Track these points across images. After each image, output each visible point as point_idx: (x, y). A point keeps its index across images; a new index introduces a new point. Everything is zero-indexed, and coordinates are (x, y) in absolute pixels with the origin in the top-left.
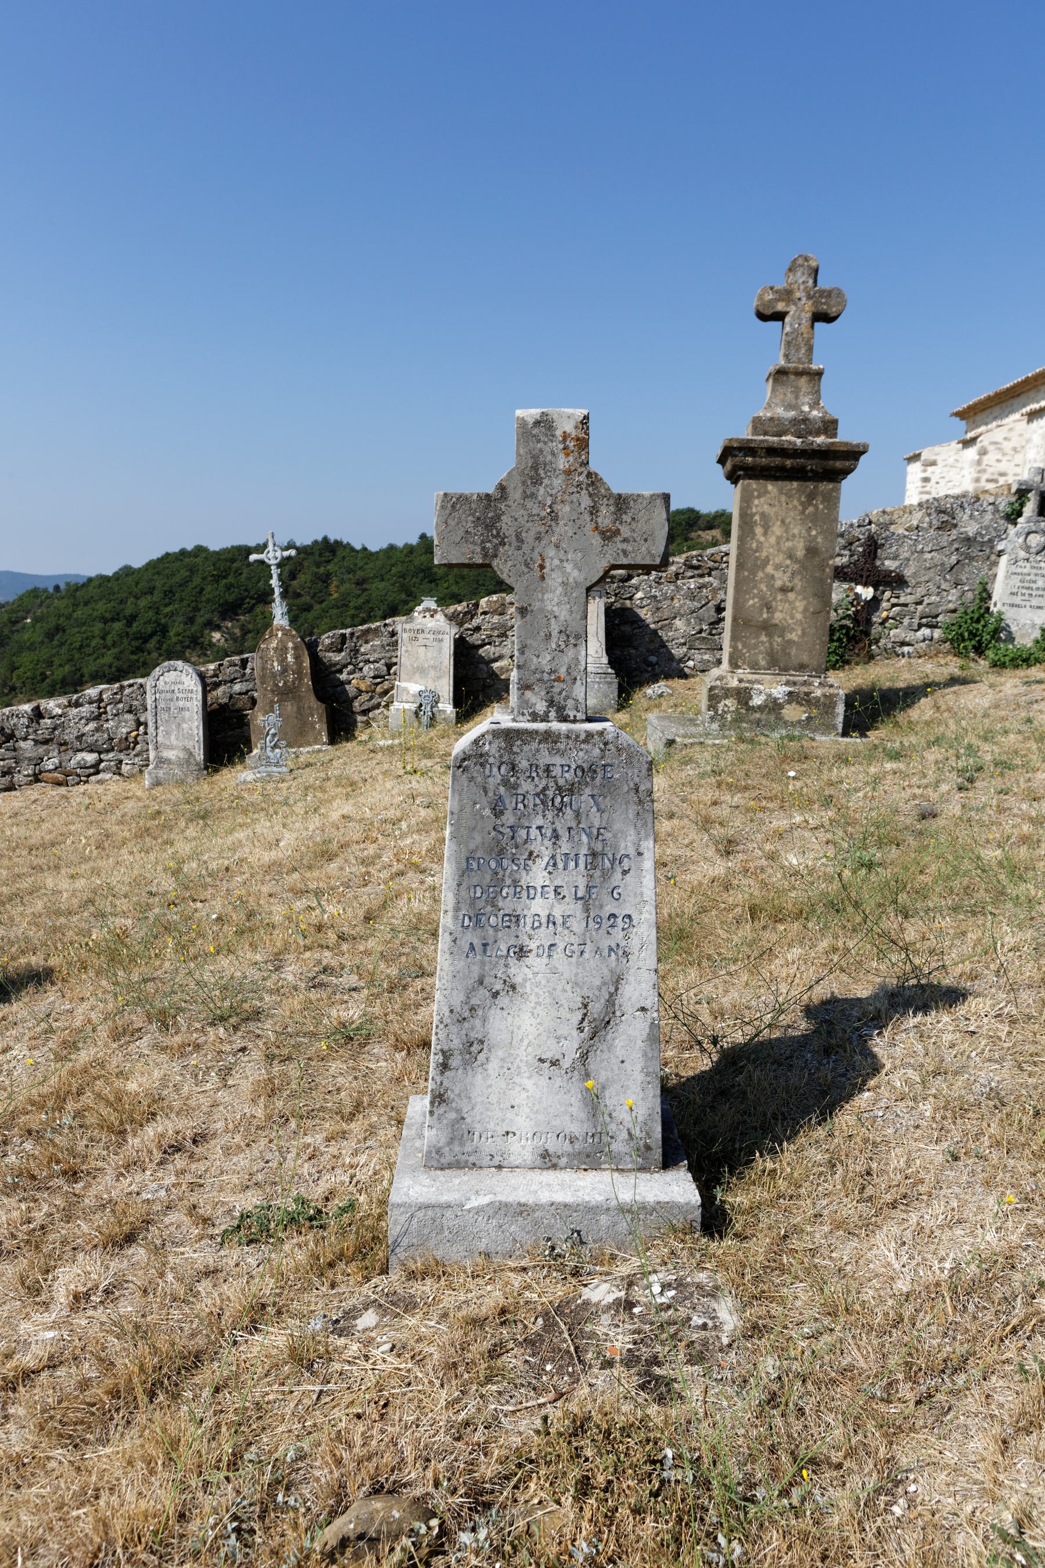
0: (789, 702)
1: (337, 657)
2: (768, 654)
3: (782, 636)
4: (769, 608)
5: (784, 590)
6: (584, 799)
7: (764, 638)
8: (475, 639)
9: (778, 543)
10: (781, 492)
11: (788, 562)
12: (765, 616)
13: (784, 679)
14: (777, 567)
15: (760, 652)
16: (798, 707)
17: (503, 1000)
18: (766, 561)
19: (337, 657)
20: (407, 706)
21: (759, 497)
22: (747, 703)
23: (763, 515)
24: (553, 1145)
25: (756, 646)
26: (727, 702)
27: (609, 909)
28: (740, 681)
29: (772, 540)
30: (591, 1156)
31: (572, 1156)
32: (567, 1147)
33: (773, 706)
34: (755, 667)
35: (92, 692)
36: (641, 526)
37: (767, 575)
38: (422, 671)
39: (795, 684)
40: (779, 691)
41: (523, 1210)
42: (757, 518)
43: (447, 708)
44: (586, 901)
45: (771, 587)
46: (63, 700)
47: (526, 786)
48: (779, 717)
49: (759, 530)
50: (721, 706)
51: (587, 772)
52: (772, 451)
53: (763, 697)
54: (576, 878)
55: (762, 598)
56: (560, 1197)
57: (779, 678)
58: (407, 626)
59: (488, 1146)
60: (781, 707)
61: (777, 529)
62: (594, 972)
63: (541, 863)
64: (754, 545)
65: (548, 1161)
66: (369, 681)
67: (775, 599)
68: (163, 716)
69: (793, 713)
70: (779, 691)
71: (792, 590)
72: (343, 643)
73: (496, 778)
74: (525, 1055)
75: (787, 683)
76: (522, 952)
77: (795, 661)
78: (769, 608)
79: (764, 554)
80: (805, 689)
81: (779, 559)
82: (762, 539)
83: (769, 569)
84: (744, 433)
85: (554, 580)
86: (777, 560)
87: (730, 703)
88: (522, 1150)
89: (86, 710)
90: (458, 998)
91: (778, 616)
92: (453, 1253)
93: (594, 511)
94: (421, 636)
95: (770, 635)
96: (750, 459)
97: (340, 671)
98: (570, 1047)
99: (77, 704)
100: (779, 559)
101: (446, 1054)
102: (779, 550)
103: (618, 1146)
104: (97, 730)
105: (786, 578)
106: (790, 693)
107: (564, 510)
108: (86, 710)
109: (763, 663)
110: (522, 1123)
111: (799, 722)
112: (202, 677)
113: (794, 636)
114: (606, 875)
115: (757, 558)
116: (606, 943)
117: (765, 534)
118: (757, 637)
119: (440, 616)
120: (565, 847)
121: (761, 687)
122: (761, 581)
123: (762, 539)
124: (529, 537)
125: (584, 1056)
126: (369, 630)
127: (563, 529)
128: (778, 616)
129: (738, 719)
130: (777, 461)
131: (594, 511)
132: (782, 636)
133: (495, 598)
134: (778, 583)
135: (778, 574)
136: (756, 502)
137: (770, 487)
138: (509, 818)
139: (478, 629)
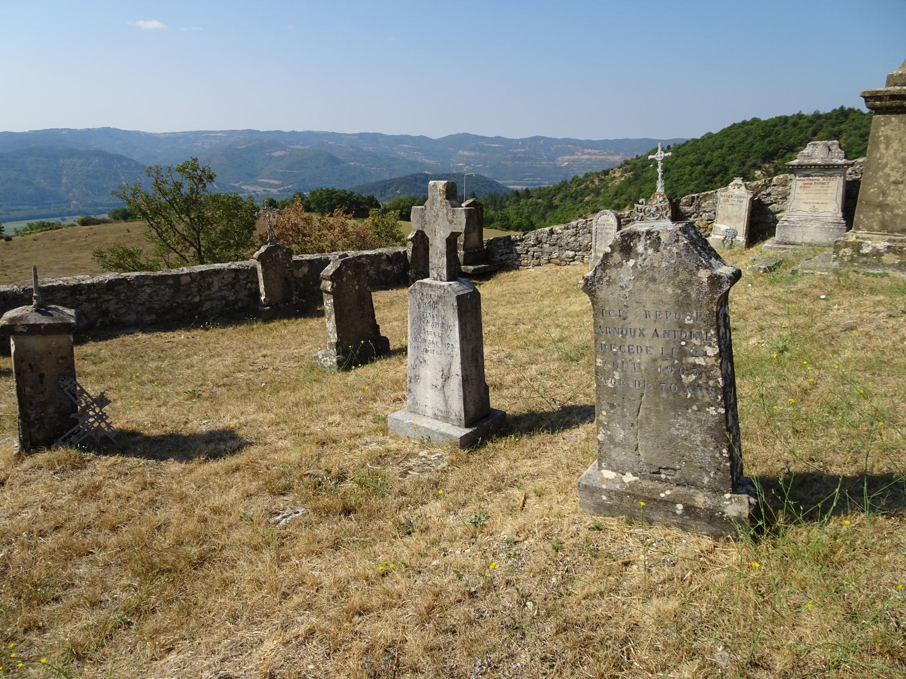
0: (887, 252)
1: (689, 209)
2: (880, 222)
3: (891, 211)
4: (884, 194)
5: (896, 183)
6: (440, 306)
7: (878, 212)
8: (767, 200)
9: (895, 154)
10: (901, 122)
11: (901, 165)
12: (881, 199)
13: (888, 237)
14: (893, 169)
15: (875, 221)
16: (893, 255)
17: (423, 364)
18: (886, 165)
19: (689, 209)
20: (717, 237)
21: (884, 126)
22: (858, 252)
23: (886, 137)
24: (438, 413)
25: (873, 217)
26: (846, 250)
27: (447, 341)
28: (857, 238)
29: (891, 152)
30: (446, 419)
31: (442, 417)
32: (440, 414)
33: (878, 253)
34: (870, 229)
35: (574, 223)
36: (459, 219)
37: (885, 174)
38: (729, 218)
39: (894, 241)
40: (882, 245)
41: (418, 427)
42: (882, 138)
43: (741, 239)
44: (441, 337)
45: (886, 181)
46: (563, 226)
47: (425, 300)
48: (879, 261)
49: (882, 146)
50: (841, 252)
51: (440, 297)
52: (893, 97)
53: (870, 248)
54: (438, 330)
55: (880, 187)
56: (427, 426)
57: (884, 237)
58: (723, 194)
59: (422, 408)
60: (882, 254)
61: (895, 145)
62: (445, 360)
63: (430, 324)
64: (878, 156)
65: (435, 417)
66: (704, 222)
67: (889, 188)
68: (599, 236)
69: (887, 258)
70: (882, 245)
71: (902, 183)
72: (693, 201)
73: (418, 297)
74: (429, 383)
75: (889, 241)
76: (427, 351)
77: (899, 228)
78: (884, 194)
79: (885, 161)
80: (901, 245)
81: (895, 163)
82: (884, 151)
83: (887, 170)
84: (881, 86)
85: (438, 236)
86: (893, 165)
87: (848, 251)
88: (429, 412)
89: (571, 231)
90: (412, 362)
91: (890, 199)
92: (401, 434)
93: (447, 214)
94: (730, 199)
95: (882, 211)
96: (878, 103)
97: (690, 216)
98: (440, 382)
99: (568, 228)
100: (895, 163)
101: (411, 378)
102: (895, 158)
103: (453, 417)
104: (575, 241)
105: (898, 176)
106: (889, 247)
107: (440, 213)
108: (571, 231)
109: (876, 227)
110: (429, 404)
111: (893, 265)
112: (619, 218)
113: (900, 212)
114: (446, 331)
115: (879, 164)
116: (447, 352)
117: (887, 148)
118: (874, 212)
119: (743, 188)
120: (436, 321)
121: (870, 242)
122: (880, 178)
123: (884, 151)
124: (432, 222)
125: (443, 387)
126: (707, 195)
127: (440, 220)
128: (890, 199)
129: (852, 260)
130: (898, 102)
131: (447, 214)
132: (891, 211)
133: (781, 176)
134: (892, 179)
135: (892, 173)
136: (882, 129)
137: (893, 119)
138: (422, 309)
139: (769, 194)
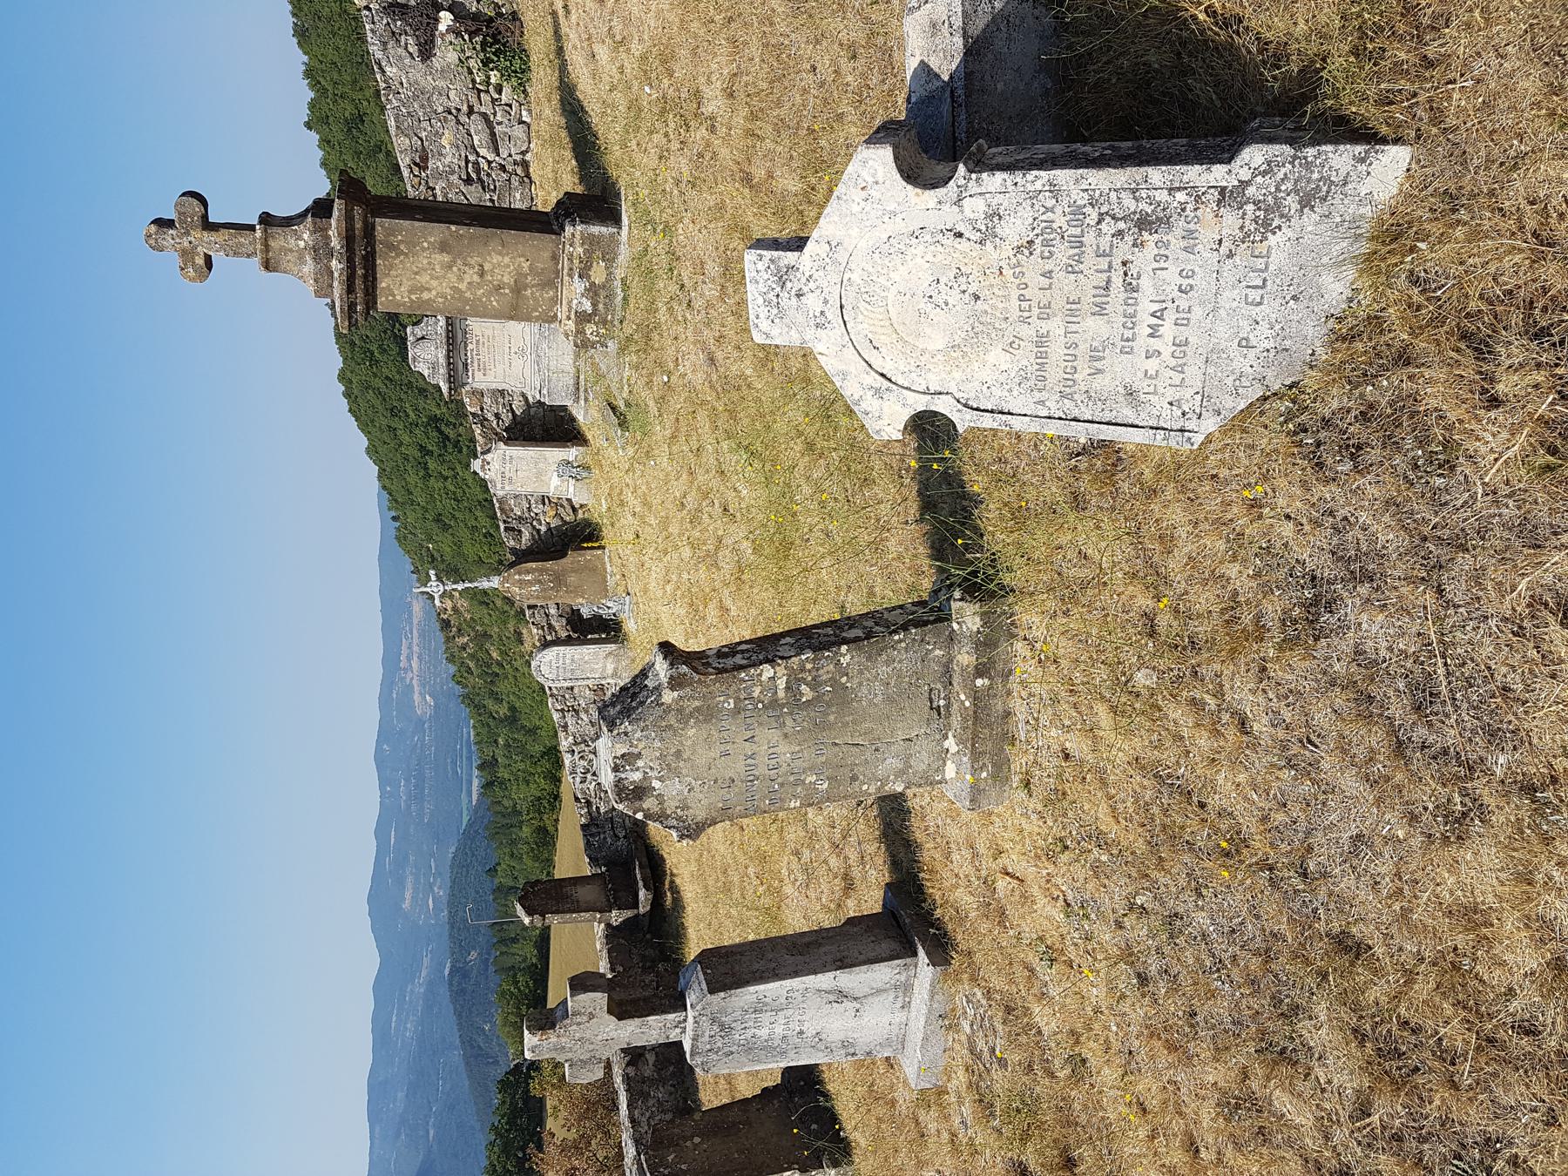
1: (526, 535)
5: (482, 274)
8: (507, 419)
13: (566, 278)
14: (460, 279)
17: (824, 1036)
19: (526, 535)
20: (571, 489)
24: (899, 1005)
25: (535, 299)
27: (783, 1000)
29: (434, 283)
30: (907, 988)
33: (593, 291)
34: (555, 301)
35: (556, 716)
38: (539, 474)
40: (579, 286)
41: (926, 1039)
43: (572, 453)
46: (561, 735)
49: (426, 296)
52: (350, 289)
54: (766, 1018)
55: (490, 293)
58: (499, 486)
61: (424, 279)
65: (906, 1006)
66: (547, 508)
68: (578, 674)
69: (598, 274)
70: (579, 286)
72: (513, 529)
73: (715, 1057)
74: (852, 1023)
75: (571, 276)
76: (801, 1032)
80: (576, 262)
83: (463, 286)
85: (613, 1034)
87: (590, 329)
88: (900, 1017)
89: (570, 720)
92: (942, 1063)
93: (579, 1024)
94: (507, 475)
95: (525, 287)
97: (538, 531)
98: (847, 1004)
99: (565, 727)
104: (587, 712)
108: (570, 720)
111: (607, 268)
112: (546, 645)
113: (526, 265)
114: (766, 1004)
117: (429, 290)
119: (488, 457)
126: (501, 509)
130: (359, 283)
131: (579, 1024)
133: (467, 400)
134: (476, 278)
139: (497, 416)
